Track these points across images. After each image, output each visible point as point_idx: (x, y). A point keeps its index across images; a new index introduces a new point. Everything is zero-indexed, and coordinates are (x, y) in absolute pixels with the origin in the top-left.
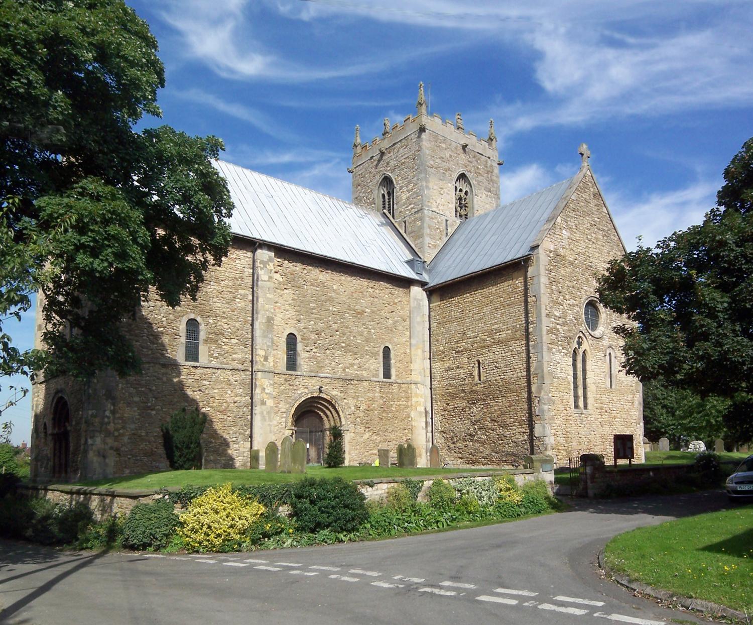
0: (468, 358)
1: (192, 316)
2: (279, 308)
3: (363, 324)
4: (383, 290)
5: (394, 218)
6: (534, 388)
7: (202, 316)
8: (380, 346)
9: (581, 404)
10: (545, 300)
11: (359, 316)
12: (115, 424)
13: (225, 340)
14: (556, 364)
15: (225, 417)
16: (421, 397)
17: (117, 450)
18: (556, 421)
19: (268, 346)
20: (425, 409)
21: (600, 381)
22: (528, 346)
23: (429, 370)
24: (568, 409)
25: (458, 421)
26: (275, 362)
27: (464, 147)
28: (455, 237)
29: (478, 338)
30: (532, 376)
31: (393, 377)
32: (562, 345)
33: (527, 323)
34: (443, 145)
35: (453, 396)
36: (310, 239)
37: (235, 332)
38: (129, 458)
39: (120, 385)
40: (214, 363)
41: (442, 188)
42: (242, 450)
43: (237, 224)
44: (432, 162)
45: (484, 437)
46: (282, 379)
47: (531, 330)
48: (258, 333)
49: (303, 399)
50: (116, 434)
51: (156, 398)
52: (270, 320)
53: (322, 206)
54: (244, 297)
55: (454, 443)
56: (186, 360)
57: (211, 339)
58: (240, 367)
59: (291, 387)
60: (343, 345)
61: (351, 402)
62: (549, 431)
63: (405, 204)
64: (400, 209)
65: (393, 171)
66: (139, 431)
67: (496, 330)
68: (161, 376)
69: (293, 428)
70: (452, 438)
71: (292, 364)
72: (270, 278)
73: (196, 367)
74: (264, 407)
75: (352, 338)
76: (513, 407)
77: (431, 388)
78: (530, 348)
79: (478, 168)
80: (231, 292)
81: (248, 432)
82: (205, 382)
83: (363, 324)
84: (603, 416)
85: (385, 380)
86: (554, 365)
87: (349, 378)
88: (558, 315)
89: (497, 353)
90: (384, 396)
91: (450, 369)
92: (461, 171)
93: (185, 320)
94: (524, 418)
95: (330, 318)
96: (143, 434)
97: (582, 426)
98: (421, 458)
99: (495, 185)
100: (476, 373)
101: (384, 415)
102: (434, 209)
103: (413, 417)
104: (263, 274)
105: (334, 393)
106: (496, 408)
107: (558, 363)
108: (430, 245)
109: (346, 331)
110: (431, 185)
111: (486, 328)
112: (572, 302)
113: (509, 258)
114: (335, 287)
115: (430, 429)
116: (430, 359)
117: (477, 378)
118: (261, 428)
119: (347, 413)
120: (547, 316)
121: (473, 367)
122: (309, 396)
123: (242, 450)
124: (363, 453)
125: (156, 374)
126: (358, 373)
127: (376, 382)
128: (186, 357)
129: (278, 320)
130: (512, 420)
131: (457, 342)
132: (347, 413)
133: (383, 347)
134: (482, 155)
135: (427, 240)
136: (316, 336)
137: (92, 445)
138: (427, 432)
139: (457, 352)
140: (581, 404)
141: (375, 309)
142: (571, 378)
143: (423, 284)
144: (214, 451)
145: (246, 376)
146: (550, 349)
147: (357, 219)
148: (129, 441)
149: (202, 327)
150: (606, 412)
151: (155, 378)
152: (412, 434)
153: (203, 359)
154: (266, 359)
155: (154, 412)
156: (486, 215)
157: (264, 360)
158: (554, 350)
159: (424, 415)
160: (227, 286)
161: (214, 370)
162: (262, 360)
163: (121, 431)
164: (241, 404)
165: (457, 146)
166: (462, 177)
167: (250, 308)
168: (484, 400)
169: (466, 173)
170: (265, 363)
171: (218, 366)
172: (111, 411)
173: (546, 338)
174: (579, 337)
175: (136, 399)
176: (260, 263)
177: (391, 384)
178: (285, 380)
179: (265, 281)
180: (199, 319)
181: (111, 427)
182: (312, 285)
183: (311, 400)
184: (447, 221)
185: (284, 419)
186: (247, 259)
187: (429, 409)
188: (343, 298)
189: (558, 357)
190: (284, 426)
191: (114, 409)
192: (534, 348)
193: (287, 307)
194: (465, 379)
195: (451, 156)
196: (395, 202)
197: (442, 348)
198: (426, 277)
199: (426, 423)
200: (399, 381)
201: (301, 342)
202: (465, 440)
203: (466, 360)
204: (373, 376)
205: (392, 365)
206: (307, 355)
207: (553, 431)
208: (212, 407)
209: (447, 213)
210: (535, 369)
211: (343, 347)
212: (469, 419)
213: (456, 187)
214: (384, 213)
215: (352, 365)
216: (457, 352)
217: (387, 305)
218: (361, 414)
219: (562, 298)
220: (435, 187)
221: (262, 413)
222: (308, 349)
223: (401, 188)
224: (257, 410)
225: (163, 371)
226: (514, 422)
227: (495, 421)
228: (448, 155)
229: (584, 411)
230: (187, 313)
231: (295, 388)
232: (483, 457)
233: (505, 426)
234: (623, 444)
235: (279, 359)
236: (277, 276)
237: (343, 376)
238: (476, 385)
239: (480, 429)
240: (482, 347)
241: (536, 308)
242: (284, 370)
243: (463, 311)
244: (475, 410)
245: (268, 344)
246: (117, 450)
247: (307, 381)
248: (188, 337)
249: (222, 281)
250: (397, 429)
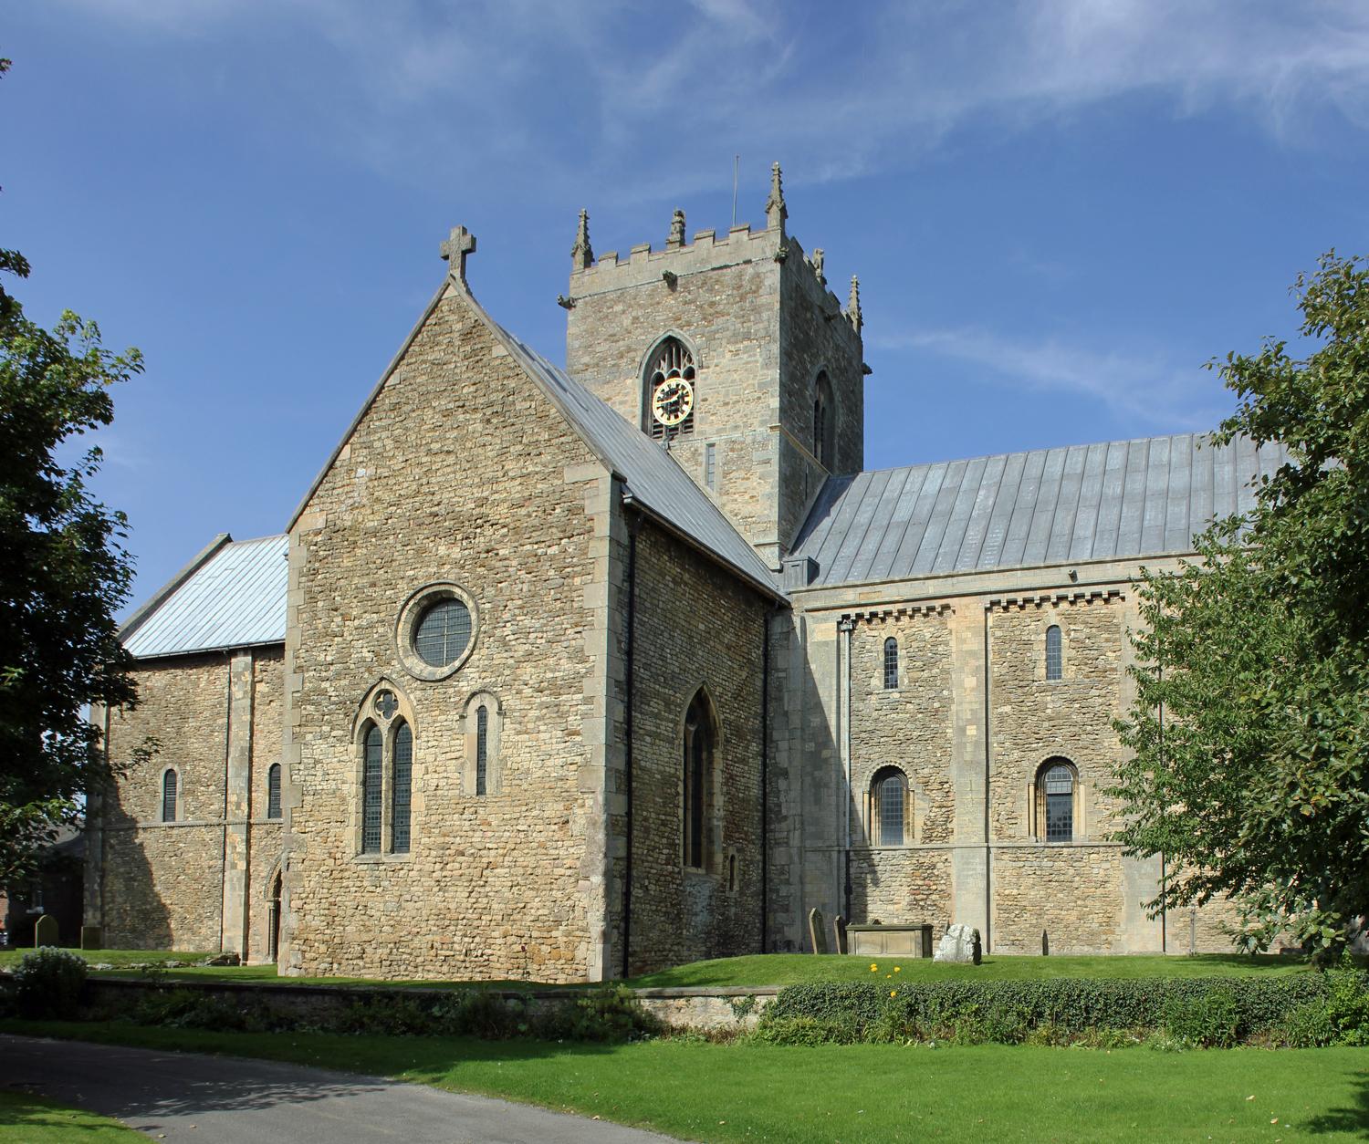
40: (191, 820)
74: (234, 871)
149: (179, 777)
153: (179, 818)
161: (188, 829)
230: (165, 763)
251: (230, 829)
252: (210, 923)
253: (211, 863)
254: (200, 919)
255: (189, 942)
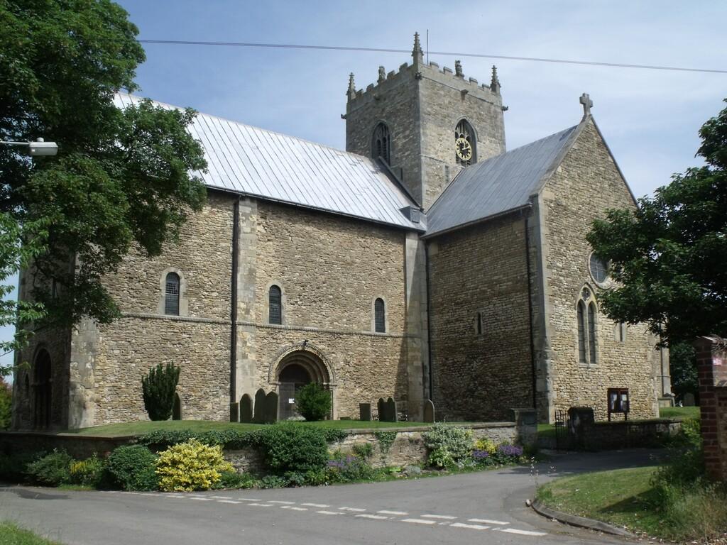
0: (468, 311)
1: (173, 270)
2: (262, 260)
3: (353, 275)
4: (376, 244)
5: (389, 165)
6: (536, 342)
7: (182, 270)
8: (372, 298)
9: (588, 357)
10: (546, 250)
11: (348, 266)
12: (94, 375)
13: (205, 293)
14: (560, 318)
15: (206, 371)
16: (418, 351)
17: (98, 401)
18: (560, 376)
19: (250, 299)
20: (423, 364)
21: (609, 334)
22: (530, 298)
23: (426, 323)
24: (573, 363)
25: (458, 377)
26: (258, 316)
27: (464, 93)
28: (456, 183)
29: (478, 290)
30: (534, 329)
31: (387, 330)
32: (565, 297)
33: (529, 274)
34: (442, 93)
35: (452, 350)
36: (296, 191)
37: (216, 285)
38: (109, 410)
39: (101, 338)
40: (194, 317)
41: (441, 135)
42: (222, 403)
43: (213, 177)
44: (429, 109)
45: (484, 393)
46: (264, 333)
47: (532, 281)
48: (240, 285)
49: (287, 353)
50: (97, 385)
51: (136, 351)
52: (252, 273)
53: (311, 156)
54: (224, 250)
55: (453, 399)
56: (166, 313)
57: (191, 292)
58: (221, 320)
59: (275, 341)
60: (331, 297)
61: (340, 357)
62: (552, 385)
63: (400, 150)
64: (396, 156)
65: (388, 118)
66: (119, 383)
67: (496, 280)
68: (140, 329)
69: (277, 382)
70: (451, 394)
71: (276, 316)
72: (253, 230)
73: (176, 321)
74: (245, 361)
75: (340, 290)
76: (514, 362)
77: (429, 342)
78: (532, 300)
79: (480, 114)
80: (212, 245)
81: (228, 386)
82: (184, 336)
83: (353, 275)
84: (612, 371)
85: (377, 333)
86: (556, 318)
87: (338, 331)
88: (561, 266)
89: (498, 305)
90: (377, 350)
91: (448, 322)
92: (461, 117)
93: (165, 274)
94: (525, 373)
95: (317, 270)
96: (123, 386)
97: (589, 380)
98: (418, 415)
99: (500, 131)
100: (476, 326)
101: (376, 370)
102: (432, 156)
103: (409, 371)
104: (244, 226)
105: (321, 346)
106: (497, 362)
107: (562, 316)
108: (429, 193)
109: (334, 282)
110: (428, 132)
111: (486, 280)
112: (576, 252)
113: (508, 207)
114: (322, 237)
115: (427, 385)
116: (428, 311)
117: (477, 331)
118: (243, 382)
119: (336, 368)
120: (548, 267)
121: (473, 320)
122: (294, 350)
123: (222, 403)
124: (354, 410)
125: (136, 327)
126: (348, 326)
127: (367, 335)
128: (166, 310)
129: (260, 273)
130: (513, 375)
131: (456, 294)
132: (336, 368)
133: (375, 298)
134: (484, 101)
135: (425, 187)
136: (302, 288)
137: (73, 396)
138: (425, 388)
139: (457, 304)
140: (588, 357)
141: (367, 259)
142: (576, 331)
143: (420, 233)
144: (194, 405)
145: (227, 330)
146: (552, 301)
147: (349, 166)
148: (109, 392)
149: (183, 280)
150: (616, 366)
151: (134, 331)
152: (408, 390)
153: (183, 313)
154: (247, 311)
155: (134, 365)
156: (488, 161)
157: (246, 314)
158: (557, 302)
159: (421, 370)
160: (208, 239)
161: (193, 324)
162: (243, 312)
163: (101, 383)
164: (221, 358)
165: (457, 93)
166: (463, 124)
167: (230, 260)
168: (485, 354)
169: (467, 119)
170: (246, 316)
171: (199, 318)
172: (91, 363)
173: (547, 290)
174: (585, 289)
175: (117, 352)
176: (242, 215)
177: (384, 338)
178: (268, 333)
179: (247, 233)
180: (179, 273)
181: (92, 378)
182: (297, 236)
183: (296, 354)
184: (447, 167)
185: (267, 373)
186: (229, 212)
187: (427, 363)
188: (331, 249)
189: (561, 309)
190: (267, 380)
191: (95, 362)
192: (535, 300)
193: (271, 259)
194: (465, 333)
195: (450, 103)
196: (391, 148)
197: (440, 300)
198: (423, 226)
199: (424, 378)
200: (393, 334)
201: (284, 294)
202: (464, 396)
203: (465, 313)
204: (364, 330)
205: (386, 317)
206: (291, 307)
207: (556, 386)
208: (191, 360)
209: (447, 159)
210: (537, 323)
211: (330, 300)
212: (469, 374)
213: (456, 134)
214: (380, 160)
215: (341, 318)
216: (457, 304)
217: (379, 255)
218: (351, 369)
219: (565, 248)
220: (434, 134)
221: (243, 367)
222: (292, 301)
223: (397, 134)
224: (239, 363)
225: (143, 323)
226: (516, 377)
227: (496, 376)
228: (447, 102)
229: (591, 365)
230: (167, 266)
231: (279, 341)
232: (483, 414)
233: (506, 381)
234: (617, 396)
235: (262, 312)
236: (260, 228)
237: (331, 329)
238: (477, 338)
239: (481, 384)
240: (482, 300)
241: (537, 259)
242: (267, 324)
243: (462, 261)
244: (475, 364)
245: (250, 296)
246: (98, 401)
247: (292, 335)
248: (168, 291)
249: (203, 234)
250: (391, 385)
251: (240, 329)
252: (217, 400)
253: (217, 352)
254: (205, 397)
255: (194, 415)
